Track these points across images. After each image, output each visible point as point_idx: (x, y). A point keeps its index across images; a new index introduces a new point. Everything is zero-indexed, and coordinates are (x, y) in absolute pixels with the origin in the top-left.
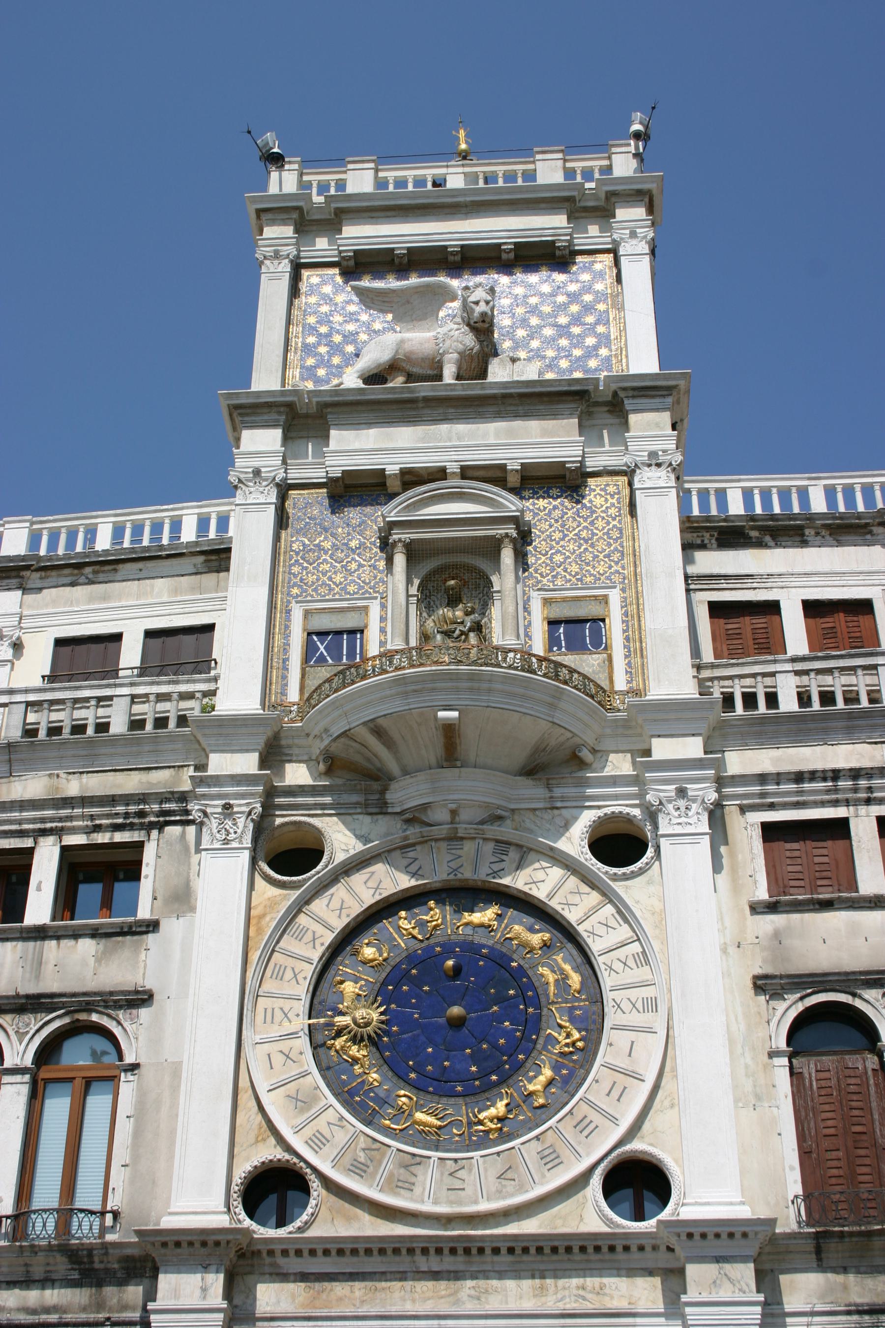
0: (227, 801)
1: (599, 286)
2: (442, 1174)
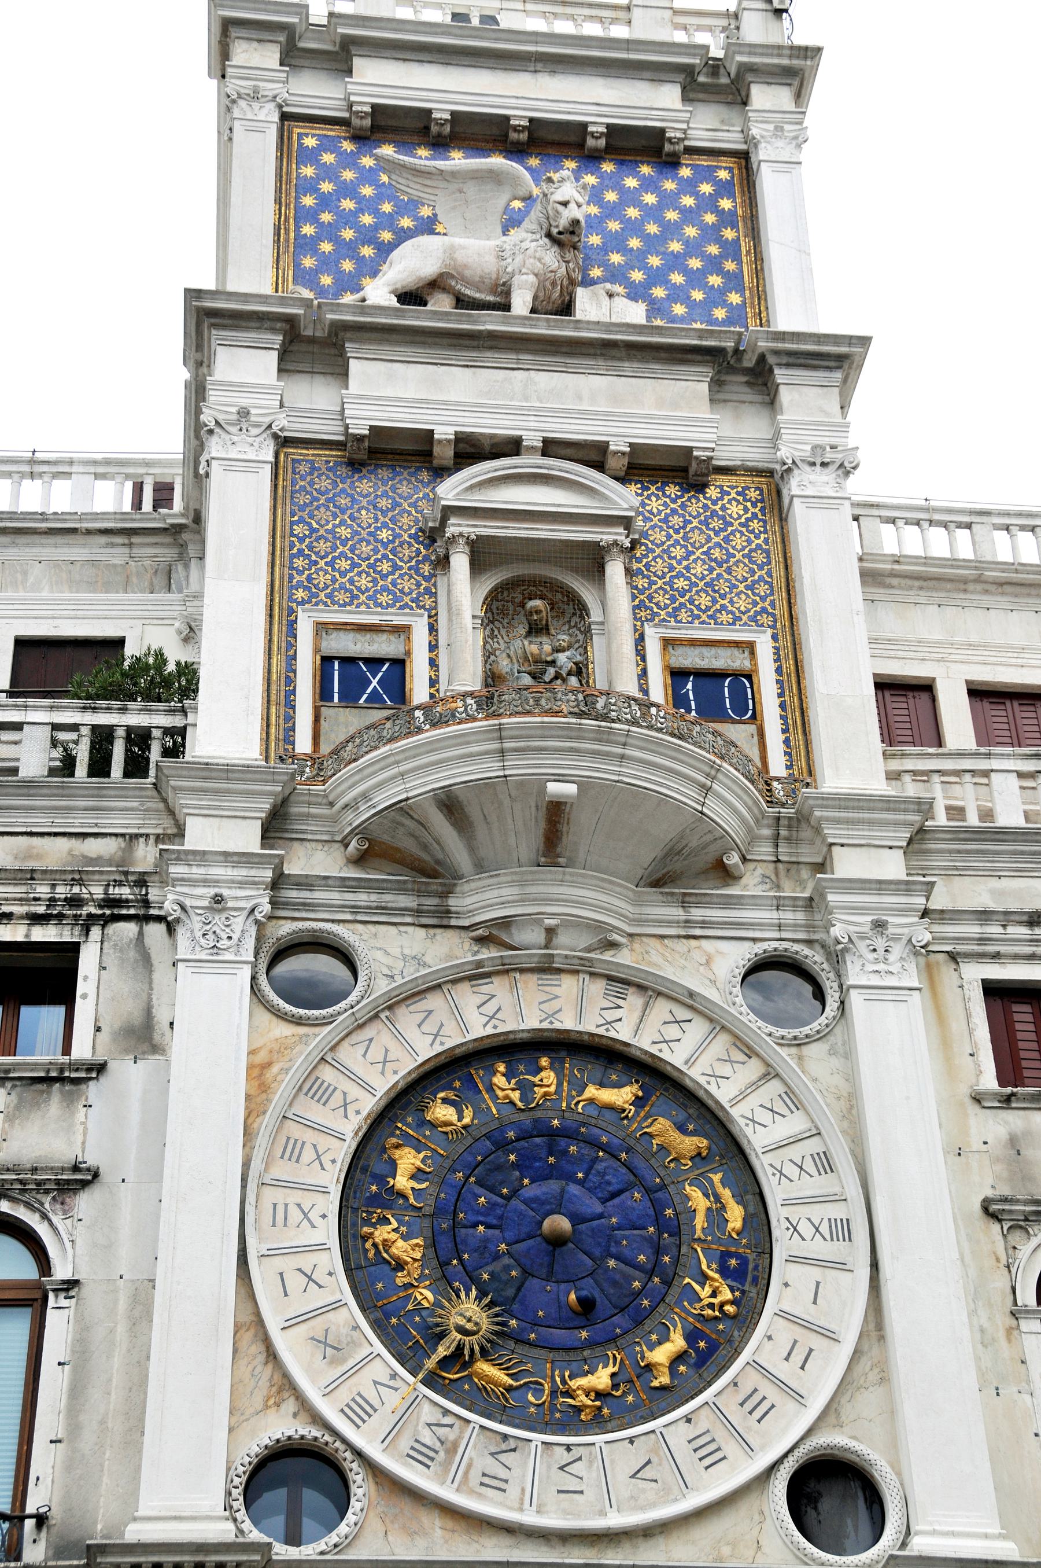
0: (217, 890)
1: (726, 204)
2: (549, 1467)
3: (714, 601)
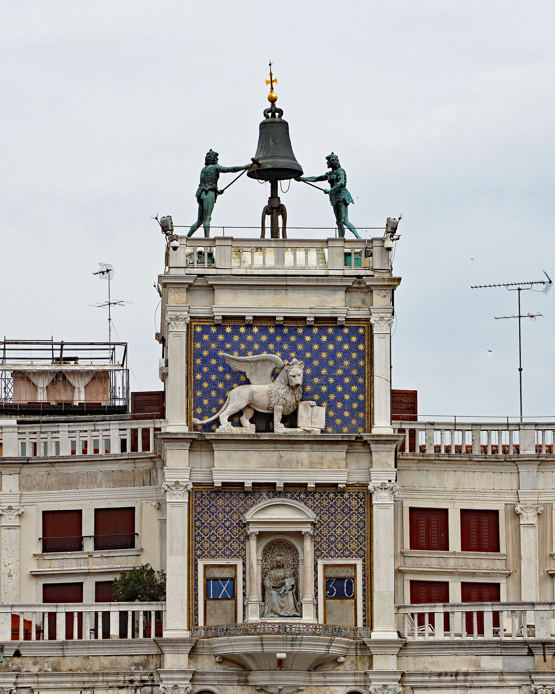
1: (361, 347)
3: (344, 546)
